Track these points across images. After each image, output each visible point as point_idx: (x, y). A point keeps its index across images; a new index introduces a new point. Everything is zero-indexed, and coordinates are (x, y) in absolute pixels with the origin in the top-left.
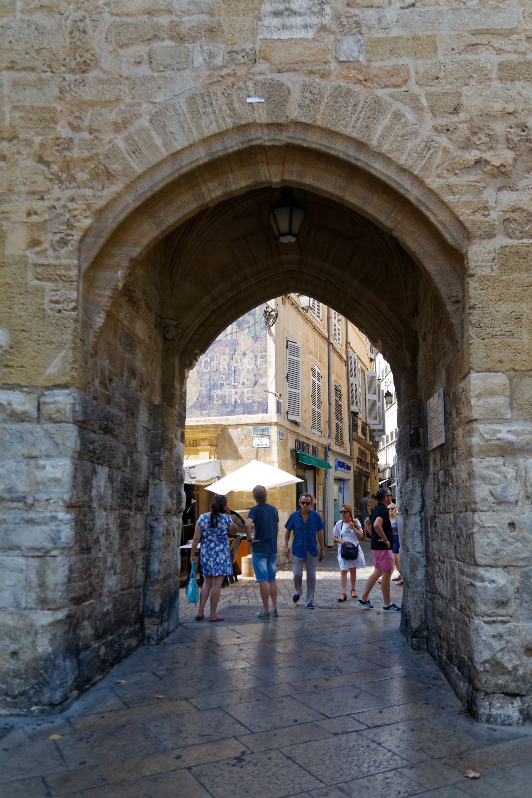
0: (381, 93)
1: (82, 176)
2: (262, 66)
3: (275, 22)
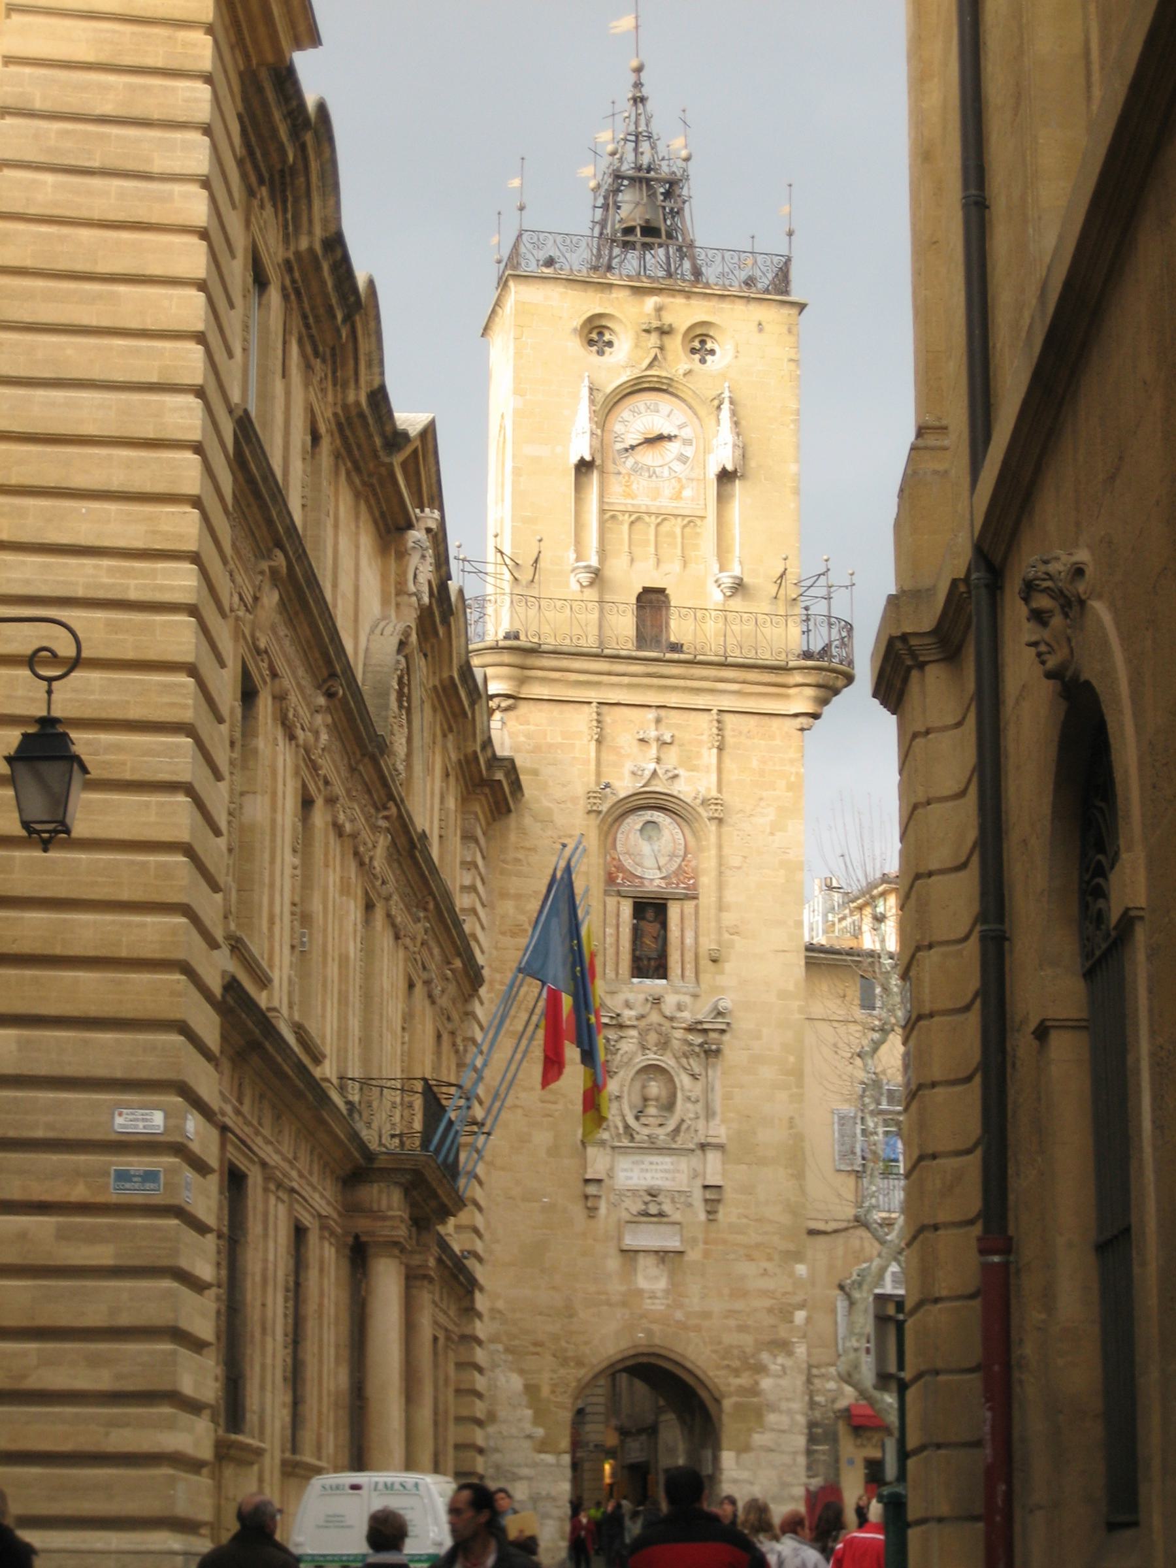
0: (692, 1334)
2: (644, 1321)
3: (648, 1301)
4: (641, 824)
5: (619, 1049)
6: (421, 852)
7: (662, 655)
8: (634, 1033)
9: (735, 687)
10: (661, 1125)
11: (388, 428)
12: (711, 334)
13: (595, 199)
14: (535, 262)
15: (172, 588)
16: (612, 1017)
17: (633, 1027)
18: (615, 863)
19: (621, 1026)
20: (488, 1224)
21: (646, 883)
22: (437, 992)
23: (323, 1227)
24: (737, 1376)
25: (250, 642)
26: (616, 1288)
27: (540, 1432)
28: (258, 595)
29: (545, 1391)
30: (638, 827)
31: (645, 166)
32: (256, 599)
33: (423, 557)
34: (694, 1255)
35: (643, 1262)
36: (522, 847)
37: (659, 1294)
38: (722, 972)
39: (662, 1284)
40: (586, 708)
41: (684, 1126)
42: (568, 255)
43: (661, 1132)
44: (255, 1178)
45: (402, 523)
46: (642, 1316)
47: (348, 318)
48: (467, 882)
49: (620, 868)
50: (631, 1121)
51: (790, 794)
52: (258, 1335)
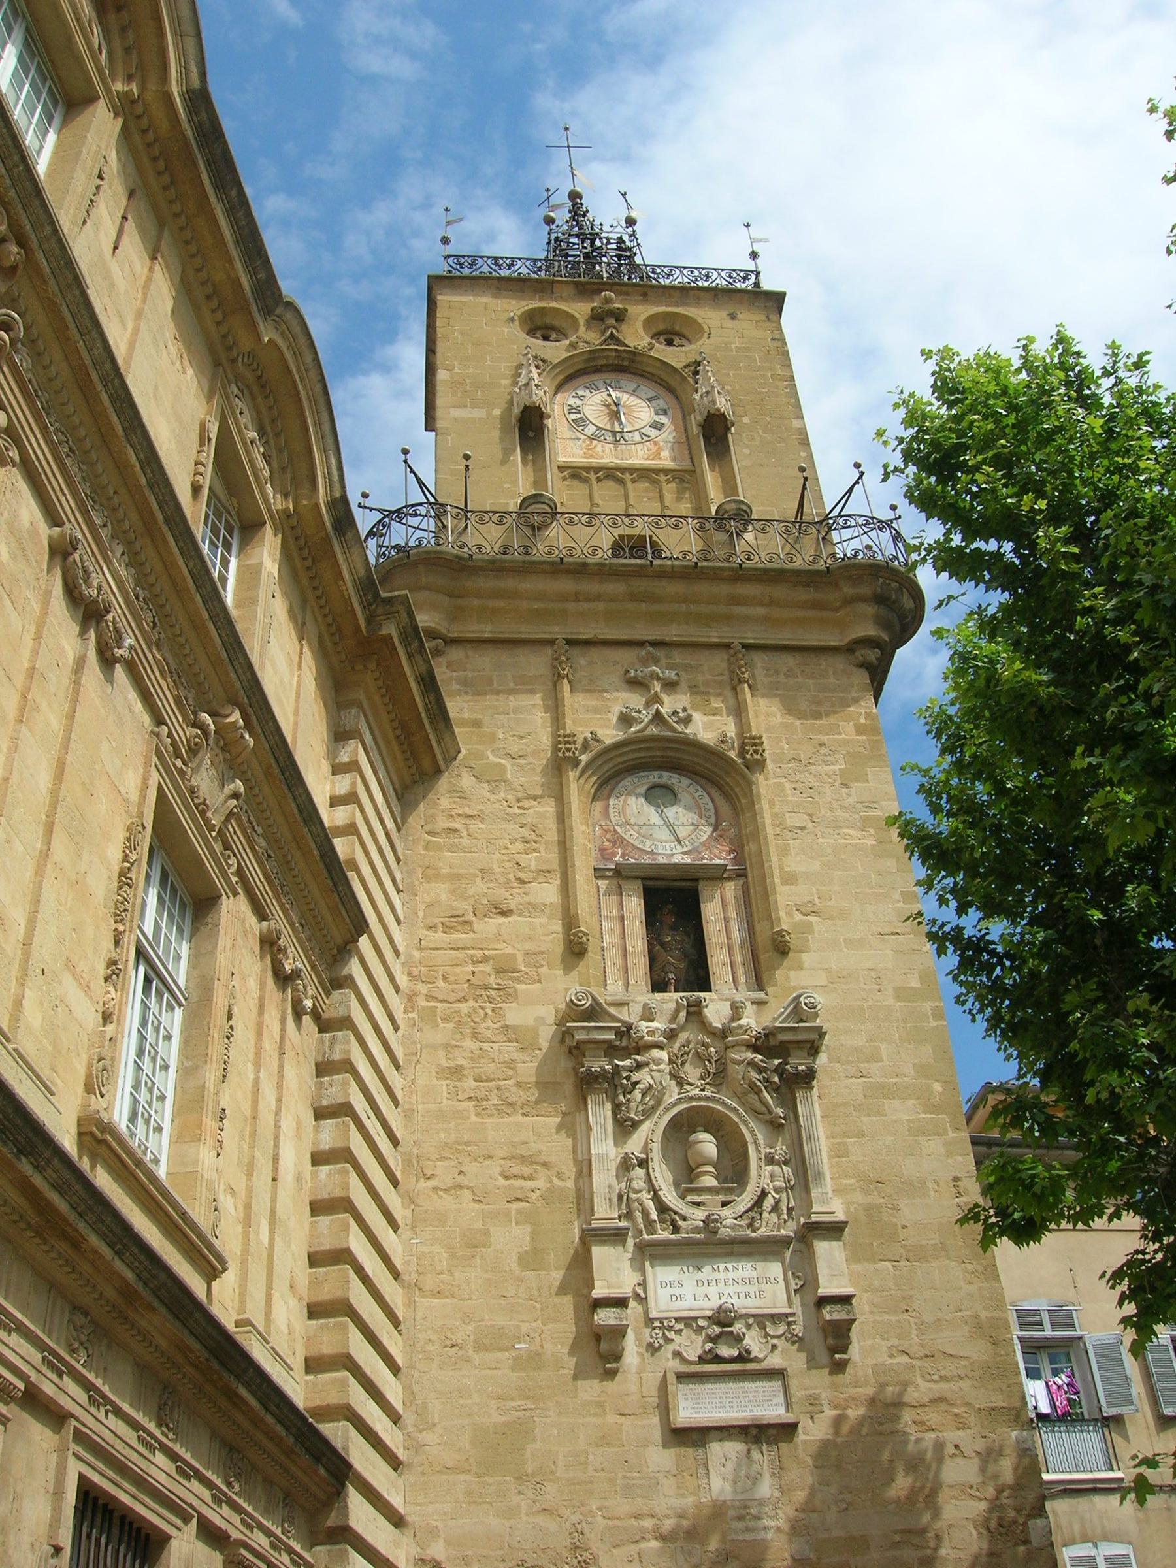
3: (739, 1525)
4: (645, 787)
5: (637, 1083)
8: (663, 1055)
9: (761, 611)
10: (724, 1204)
12: (677, 328)
16: (619, 1033)
17: (660, 1047)
18: (608, 836)
30: (643, 790)
36: (459, 815)
38: (800, 967)
40: (548, 651)
41: (769, 1202)
49: (618, 841)
50: (670, 1196)
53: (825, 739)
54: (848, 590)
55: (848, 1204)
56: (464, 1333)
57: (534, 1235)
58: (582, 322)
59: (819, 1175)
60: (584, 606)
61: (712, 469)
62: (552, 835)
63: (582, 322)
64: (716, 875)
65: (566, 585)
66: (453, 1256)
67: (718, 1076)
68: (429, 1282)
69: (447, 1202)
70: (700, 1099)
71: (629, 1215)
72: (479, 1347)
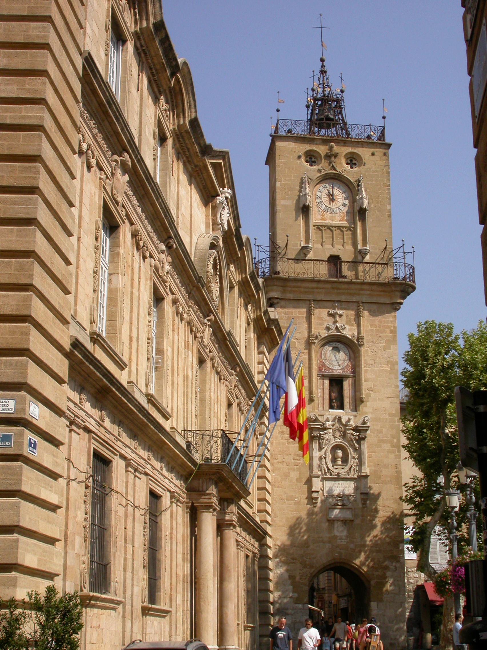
1: (308, 567)
3: (340, 541)
6: (230, 342)
7: (338, 280)
8: (331, 431)
9: (368, 292)
11: (201, 142)
13: (308, 111)
14: (284, 131)
15: (30, 117)
16: (321, 425)
17: (330, 429)
19: (325, 429)
20: (272, 510)
21: (334, 371)
22: (245, 408)
23: (172, 497)
24: (377, 571)
25: (110, 194)
26: (326, 535)
27: (296, 595)
28: (114, 172)
29: (298, 578)
31: (327, 95)
32: (112, 174)
33: (224, 208)
34: (358, 521)
35: (336, 525)
37: (344, 538)
38: (366, 406)
39: (345, 533)
41: (353, 469)
42: (297, 128)
43: (343, 470)
44: (118, 464)
45: (214, 194)
46: (337, 547)
47: (173, 74)
48: (260, 370)
49: (324, 365)
50: (330, 466)
51: (392, 334)
52: (120, 543)
53: (381, 335)
54: (393, 288)
55: (370, 469)
56: (284, 496)
57: (300, 474)
58: (323, 157)
59: (365, 463)
60: (319, 290)
61: (359, 221)
62: (307, 365)
63: (323, 157)
64: (347, 377)
65: (315, 285)
66: (282, 478)
67: (344, 435)
68: (277, 484)
69: (280, 465)
70: (339, 442)
71: (321, 470)
72: (287, 500)
